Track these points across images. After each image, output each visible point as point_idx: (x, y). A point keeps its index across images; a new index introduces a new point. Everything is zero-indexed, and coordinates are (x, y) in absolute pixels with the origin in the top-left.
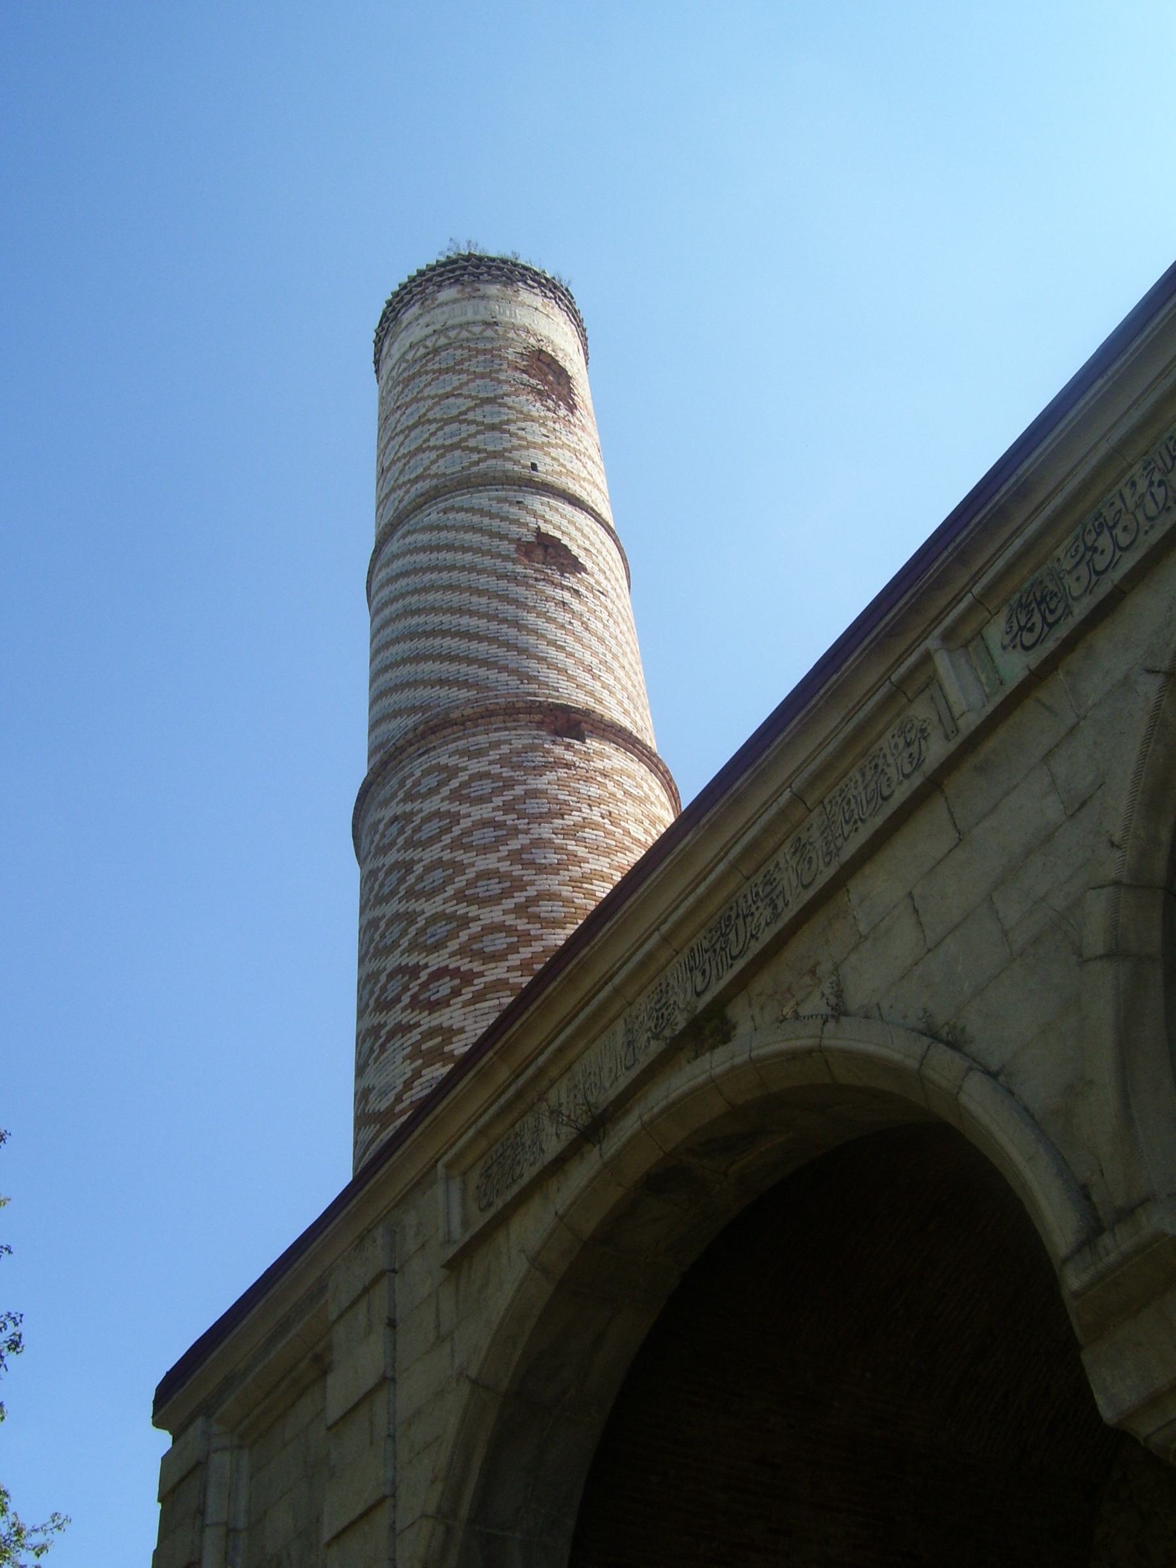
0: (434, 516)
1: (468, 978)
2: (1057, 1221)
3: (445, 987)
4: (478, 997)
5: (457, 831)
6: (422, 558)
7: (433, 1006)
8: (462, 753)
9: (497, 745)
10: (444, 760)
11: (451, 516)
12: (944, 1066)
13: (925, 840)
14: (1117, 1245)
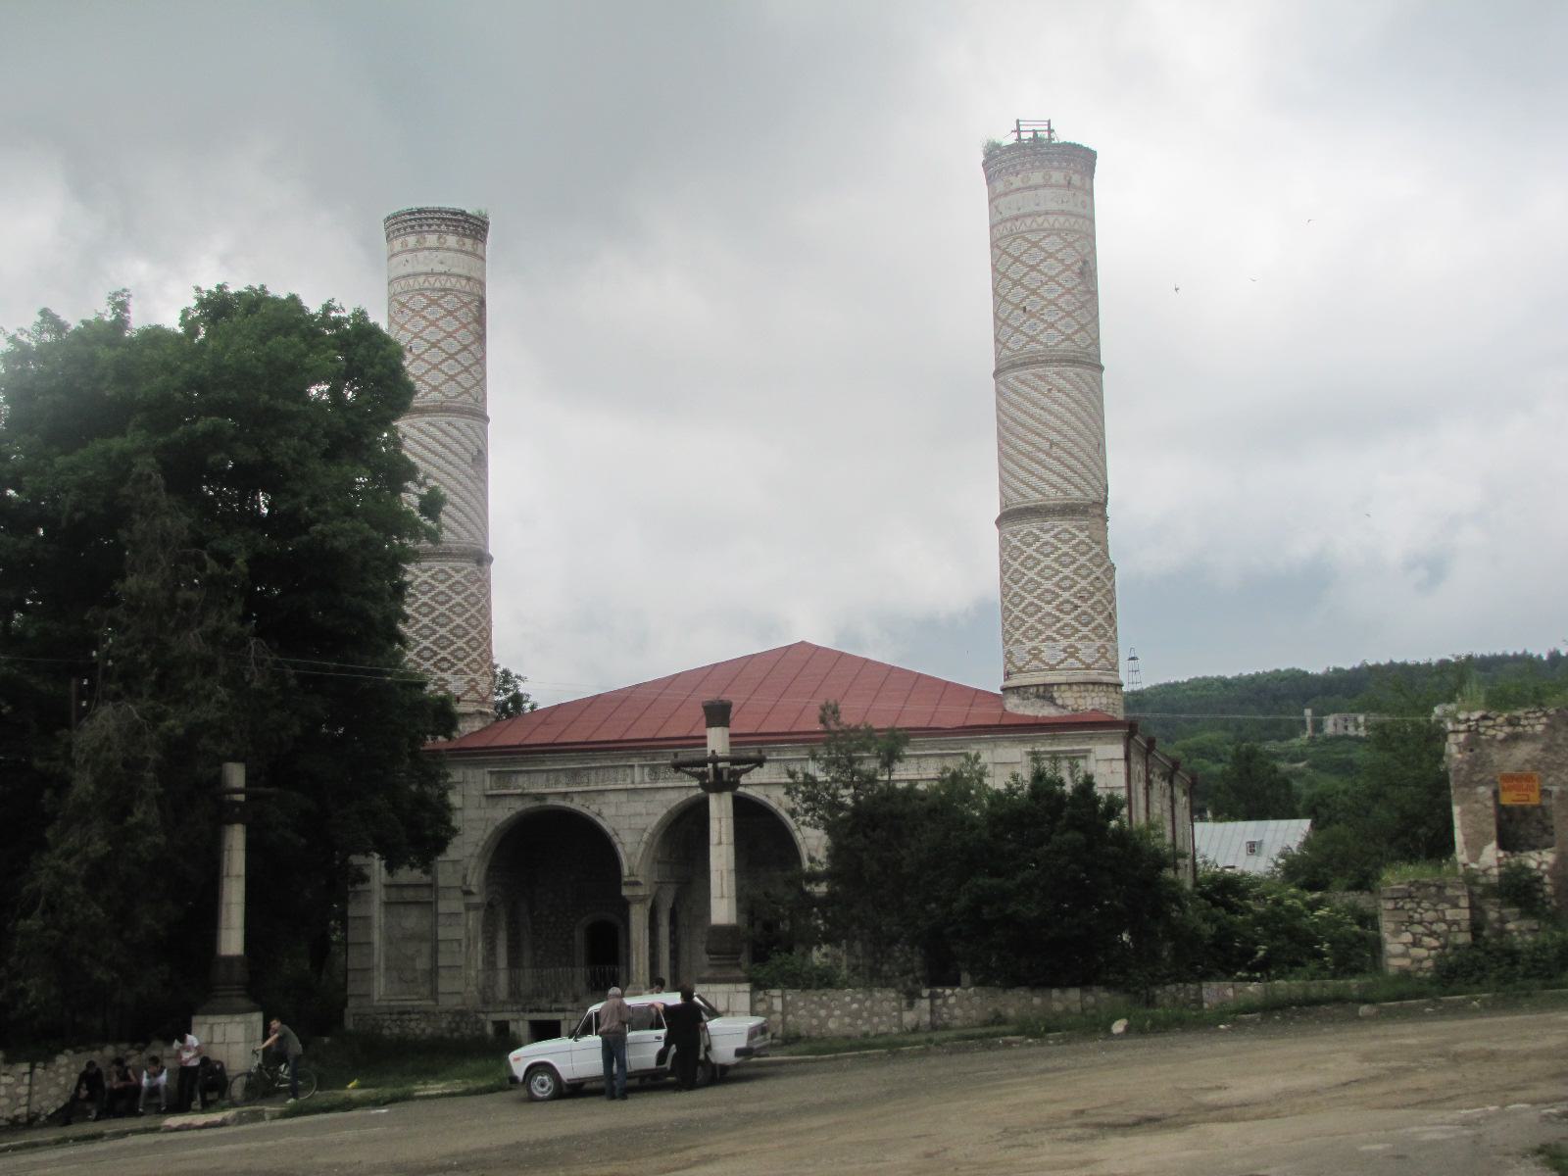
0: (444, 426)
1: (453, 665)
2: (626, 871)
3: (445, 665)
4: (455, 673)
5: (451, 604)
6: (439, 449)
7: (443, 670)
8: (453, 569)
9: (463, 569)
10: (447, 569)
11: (450, 428)
12: (615, 839)
13: (623, 797)
14: (633, 879)
